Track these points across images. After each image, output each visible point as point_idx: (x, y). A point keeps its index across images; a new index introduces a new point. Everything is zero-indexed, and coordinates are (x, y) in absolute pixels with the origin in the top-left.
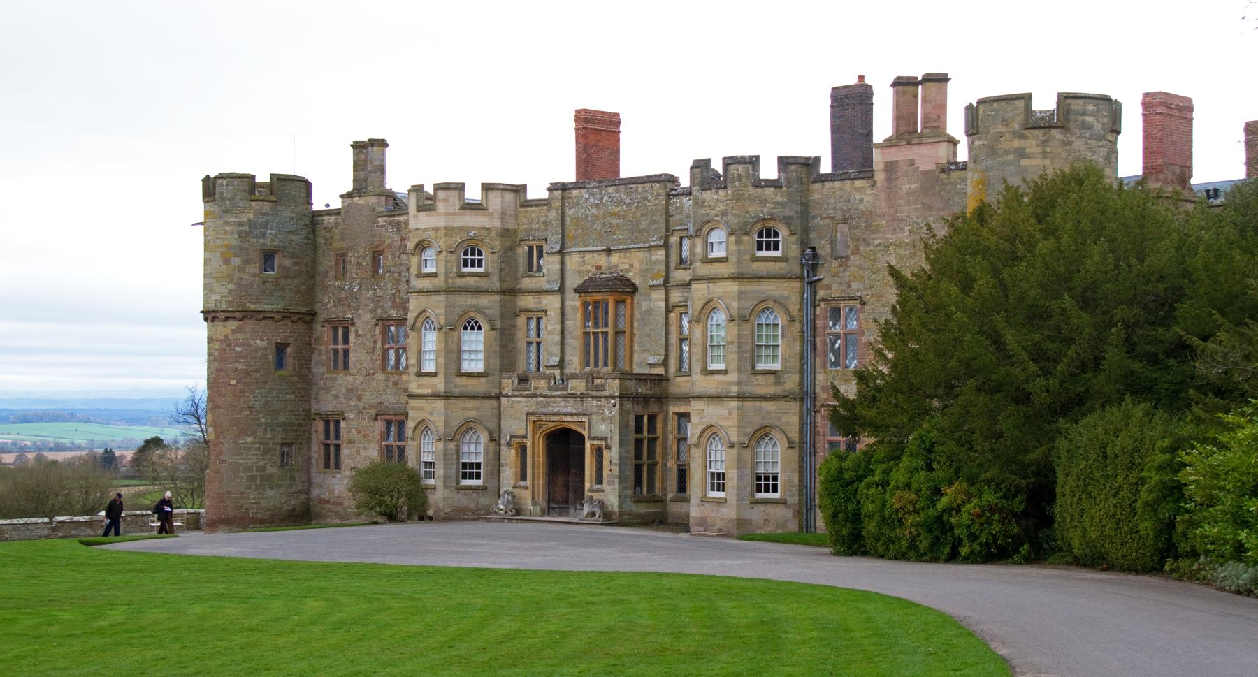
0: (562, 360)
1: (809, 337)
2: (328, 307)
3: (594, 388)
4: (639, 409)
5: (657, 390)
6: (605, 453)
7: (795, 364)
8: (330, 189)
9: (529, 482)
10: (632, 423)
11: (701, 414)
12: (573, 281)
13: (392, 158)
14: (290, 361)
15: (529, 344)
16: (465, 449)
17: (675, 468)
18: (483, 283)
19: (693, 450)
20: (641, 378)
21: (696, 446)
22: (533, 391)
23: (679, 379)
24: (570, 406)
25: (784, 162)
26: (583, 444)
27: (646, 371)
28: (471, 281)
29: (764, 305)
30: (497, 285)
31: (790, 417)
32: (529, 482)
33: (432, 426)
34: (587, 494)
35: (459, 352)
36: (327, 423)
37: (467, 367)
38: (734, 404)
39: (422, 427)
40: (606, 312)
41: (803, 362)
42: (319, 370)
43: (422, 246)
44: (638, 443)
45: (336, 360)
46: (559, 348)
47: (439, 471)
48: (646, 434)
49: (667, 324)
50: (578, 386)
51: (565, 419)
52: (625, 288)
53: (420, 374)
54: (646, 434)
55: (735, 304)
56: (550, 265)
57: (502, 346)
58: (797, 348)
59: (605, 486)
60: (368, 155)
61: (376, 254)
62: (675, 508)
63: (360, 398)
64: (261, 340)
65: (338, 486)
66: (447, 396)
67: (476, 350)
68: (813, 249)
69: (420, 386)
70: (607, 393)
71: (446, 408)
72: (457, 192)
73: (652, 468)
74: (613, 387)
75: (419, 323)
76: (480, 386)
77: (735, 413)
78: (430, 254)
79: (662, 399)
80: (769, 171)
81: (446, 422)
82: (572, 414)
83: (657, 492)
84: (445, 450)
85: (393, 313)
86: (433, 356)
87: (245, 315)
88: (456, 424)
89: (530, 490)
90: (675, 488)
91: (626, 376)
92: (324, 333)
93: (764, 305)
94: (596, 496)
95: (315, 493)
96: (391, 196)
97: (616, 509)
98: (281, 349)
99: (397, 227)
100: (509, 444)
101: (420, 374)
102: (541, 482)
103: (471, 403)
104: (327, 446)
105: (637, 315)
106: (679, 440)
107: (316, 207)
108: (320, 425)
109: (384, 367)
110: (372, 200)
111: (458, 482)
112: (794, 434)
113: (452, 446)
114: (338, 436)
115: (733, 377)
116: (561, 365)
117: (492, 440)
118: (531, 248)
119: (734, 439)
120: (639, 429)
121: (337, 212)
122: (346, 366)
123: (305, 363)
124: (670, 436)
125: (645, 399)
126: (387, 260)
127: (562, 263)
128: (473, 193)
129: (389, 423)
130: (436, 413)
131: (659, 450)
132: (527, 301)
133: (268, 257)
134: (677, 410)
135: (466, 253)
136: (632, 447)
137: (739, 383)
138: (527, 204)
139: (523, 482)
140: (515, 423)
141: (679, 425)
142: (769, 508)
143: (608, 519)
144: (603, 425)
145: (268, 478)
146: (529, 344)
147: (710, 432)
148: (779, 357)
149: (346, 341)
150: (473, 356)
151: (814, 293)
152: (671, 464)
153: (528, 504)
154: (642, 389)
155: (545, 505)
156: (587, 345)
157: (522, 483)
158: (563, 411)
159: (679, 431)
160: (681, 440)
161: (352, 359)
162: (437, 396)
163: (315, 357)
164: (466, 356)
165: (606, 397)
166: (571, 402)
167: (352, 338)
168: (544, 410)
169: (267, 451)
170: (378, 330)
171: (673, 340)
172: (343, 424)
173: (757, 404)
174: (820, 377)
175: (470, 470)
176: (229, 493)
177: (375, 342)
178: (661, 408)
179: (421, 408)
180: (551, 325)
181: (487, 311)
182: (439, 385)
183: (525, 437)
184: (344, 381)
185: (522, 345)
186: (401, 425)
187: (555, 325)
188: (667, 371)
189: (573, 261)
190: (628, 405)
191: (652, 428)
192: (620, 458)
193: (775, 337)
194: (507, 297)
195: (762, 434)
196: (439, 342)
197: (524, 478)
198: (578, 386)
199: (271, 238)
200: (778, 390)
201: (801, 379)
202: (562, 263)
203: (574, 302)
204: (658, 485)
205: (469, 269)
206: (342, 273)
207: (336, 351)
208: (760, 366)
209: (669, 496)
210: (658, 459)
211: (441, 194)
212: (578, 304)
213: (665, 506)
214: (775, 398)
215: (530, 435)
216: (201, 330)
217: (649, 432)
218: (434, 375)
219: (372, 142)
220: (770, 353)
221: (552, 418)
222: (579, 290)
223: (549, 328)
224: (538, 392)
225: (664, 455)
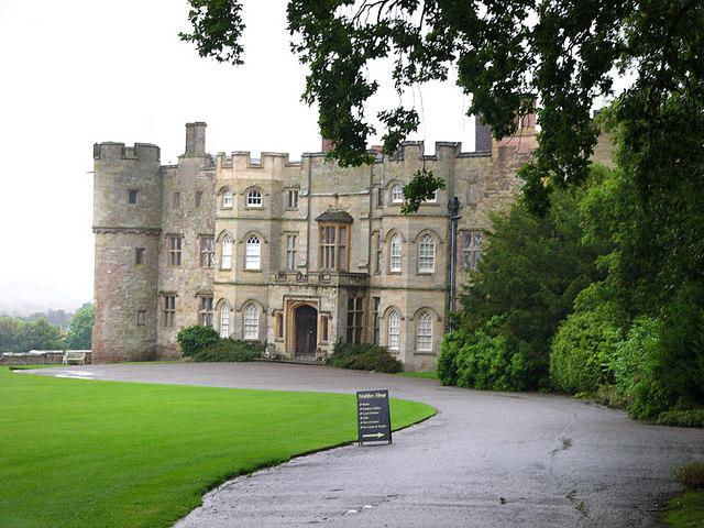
0: (308, 263)
1: (452, 251)
2: (170, 226)
3: (321, 284)
5: (362, 283)
7: (444, 267)
8: (171, 154)
9: (284, 338)
10: (346, 304)
11: (387, 299)
12: (315, 214)
13: (209, 134)
14: (144, 260)
15: (289, 252)
18: (260, 214)
20: (354, 276)
21: (383, 318)
24: (310, 292)
25: (439, 145)
27: (358, 271)
28: (253, 213)
29: (425, 233)
30: (268, 214)
31: (438, 302)
32: (284, 338)
36: (167, 298)
37: (249, 266)
38: (405, 293)
39: (221, 303)
40: (334, 233)
41: (449, 267)
42: (163, 265)
43: (224, 190)
44: (350, 316)
45: (173, 260)
49: (370, 242)
50: (314, 279)
52: (345, 220)
53: (221, 270)
55: (407, 232)
56: (302, 204)
58: (444, 259)
60: (195, 131)
61: (199, 194)
63: (187, 283)
64: (127, 245)
65: (171, 337)
66: (236, 284)
67: (255, 255)
68: (456, 198)
70: (332, 284)
72: (244, 159)
75: (221, 237)
76: (257, 278)
77: (405, 299)
78: (228, 196)
79: (366, 288)
80: (430, 150)
85: (209, 231)
86: (229, 259)
87: (117, 230)
91: (343, 273)
92: (166, 242)
93: (425, 233)
95: (159, 342)
96: (209, 157)
98: (139, 252)
99: (211, 177)
101: (221, 270)
102: (291, 338)
103: (252, 288)
104: (167, 313)
105: (353, 236)
107: (164, 162)
108: (163, 299)
109: (201, 265)
110: (197, 160)
112: (442, 313)
113: (239, 314)
114: (173, 307)
115: (405, 276)
116: (307, 266)
117: (264, 311)
118: (291, 192)
119: (405, 315)
120: (351, 306)
121: (176, 167)
122: (179, 264)
123: (155, 261)
126: (205, 196)
127: (309, 202)
128: (256, 156)
129: (204, 299)
130: (229, 294)
132: (289, 226)
133: (133, 194)
135: (250, 195)
136: (346, 319)
137: (409, 280)
138: (289, 165)
142: (425, 358)
143: (329, 362)
144: (329, 303)
145: (131, 332)
146: (289, 252)
147: (391, 310)
148: (434, 266)
149: (179, 248)
150: (253, 259)
151: (456, 226)
152: (371, 329)
156: (322, 258)
158: (305, 293)
161: (182, 260)
162: (231, 284)
163: (161, 257)
164: (249, 259)
167: (183, 245)
169: (129, 315)
170: (198, 241)
171: (374, 252)
172: (176, 299)
173: (423, 293)
174: (458, 278)
176: (106, 340)
180: (302, 241)
181: (262, 232)
182: (233, 277)
184: (177, 271)
185: (284, 252)
186: (211, 300)
187: (305, 246)
189: (316, 202)
190: (344, 292)
193: (432, 252)
194: (275, 223)
195: (422, 312)
197: (281, 336)
199: (134, 182)
200: (433, 286)
201: (448, 279)
202: (309, 202)
203: (315, 226)
205: (252, 205)
206: (177, 204)
207: (173, 253)
208: (421, 270)
211: (235, 158)
212: (317, 228)
214: (430, 290)
216: (91, 239)
219: (198, 124)
220: (428, 262)
222: (319, 220)
223: (301, 243)
224: (291, 283)
225: (366, 324)
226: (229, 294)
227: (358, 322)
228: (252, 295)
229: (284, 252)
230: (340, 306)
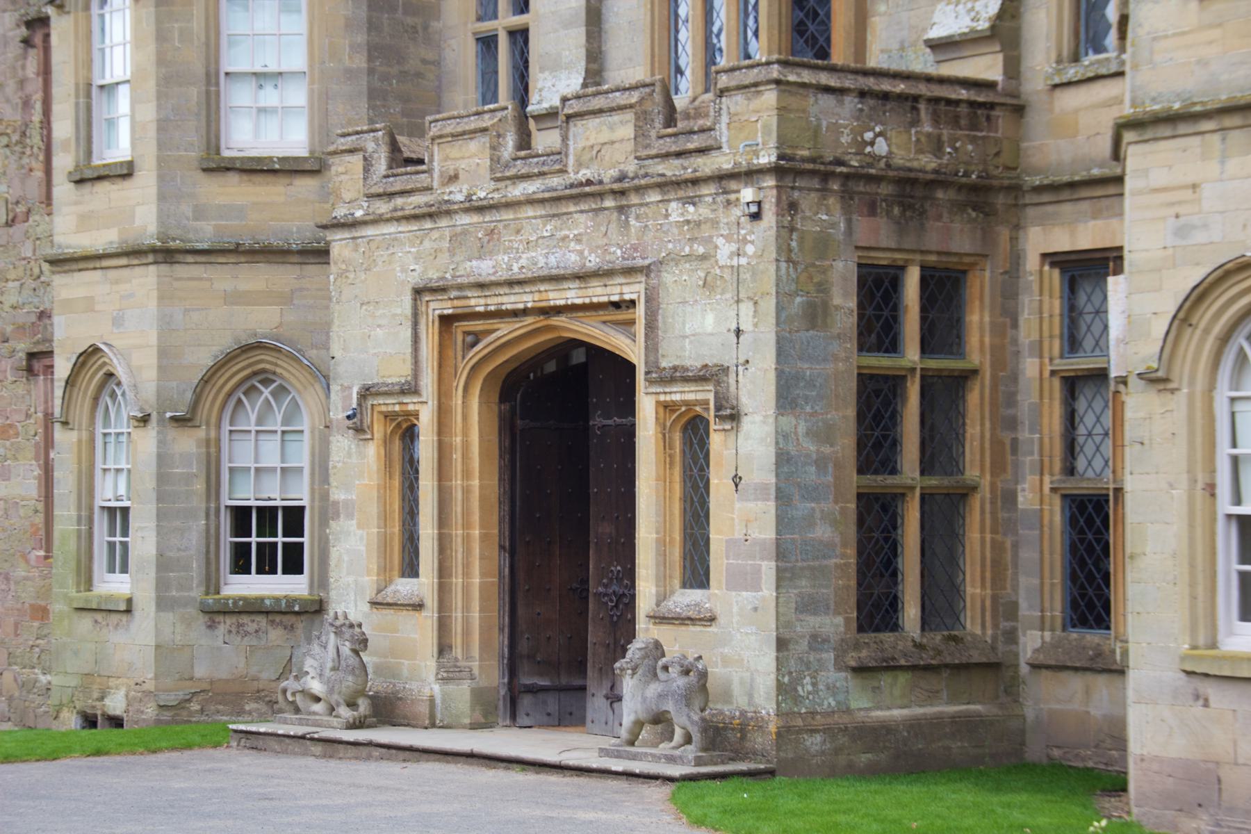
4: (878, 234)
5: (963, 152)
6: (716, 440)
9: (424, 585)
10: (844, 301)
16: (241, 454)
17: (1055, 515)
19: (1139, 406)
20: (893, 96)
21: (1157, 380)
23: (1071, 100)
24: (576, 242)
26: (628, 406)
27: (923, 63)
33: (121, 372)
34: (646, 631)
35: (213, 80)
37: (245, 136)
44: (876, 400)
46: (578, 35)
47: (143, 541)
48: (911, 353)
50: (607, 145)
51: (557, 297)
54: (911, 353)
57: (374, 51)
59: (715, 597)
62: (1056, 700)
69: (86, 221)
70: (722, 162)
71: (164, 297)
73: (945, 512)
74: (750, 129)
76: (282, 211)
79: (994, 196)
81: (163, 353)
82: (582, 277)
83: (974, 624)
84: (162, 459)
88: (204, 358)
89: (428, 618)
90: (1056, 607)
94: (677, 643)
97: (765, 703)
106: (1073, 385)
111: (212, 583)
113: (187, 443)
120: (878, 326)
124: (1030, 367)
125: (910, 193)
131: (976, 428)
134: (1062, 241)
136: (844, 416)
139: (403, 586)
140: (371, 326)
141: (1072, 314)
144: (717, 310)
150: (269, 96)
152: (1038, 497)
153: (423, 678)
154: (890, 145)
155: (493, 677)
157: (404, 588)
158: (540, 256)
159: (1073, 343)
160: (1084, 385)
162: (134, 253)
164: (239, 96)
165: (721, 178)
166: (580, 222)
168: (484, 268)
175: (270, 536)
177: (27, 104)
178: (987, 237)
179: (89, 305)
182: (138, 211)
183: (410, 389)
188: (1013, 67)
190: (824, 214)
191: (942, 329)
192: (783, 459)
196: (137, 43)
197: (411, 569)
198: (607, 145)
204: (974, 589)
209: (1031, 642)
210: (974, 469)
213: (1012, 689)
217: (926, 348)
218: (126, 172)
225: (1004, 455)
226: (127, 323)
227: (940, 448)
228: (261, 320)
229: (461, 55)
230: (801, 316)
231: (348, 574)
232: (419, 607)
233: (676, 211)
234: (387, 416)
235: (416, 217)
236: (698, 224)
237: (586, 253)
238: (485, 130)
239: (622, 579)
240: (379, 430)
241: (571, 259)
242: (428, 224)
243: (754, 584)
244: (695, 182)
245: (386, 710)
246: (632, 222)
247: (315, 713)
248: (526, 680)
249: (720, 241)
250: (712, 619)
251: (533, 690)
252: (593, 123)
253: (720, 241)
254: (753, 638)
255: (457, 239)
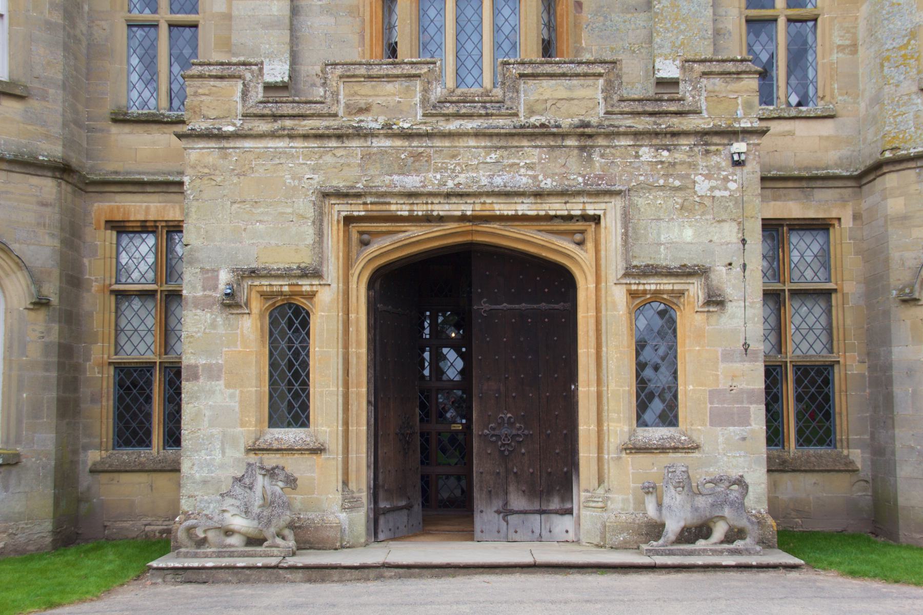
22: (345, 120)
24: (530, 167)
82: (564, 194)
100: (231, 302)
143: (684, 545)
168: (412, 182)
215: (332, 270)
221: (440, 208)
231: (211, 425)
232: (318, 451)
233: (646, 153)
234: (265, 296)
235: (305, 137)
236: (673, 165)
237: (541, 177)
238: (418, 76)
239: (514, 423)
240: (256, 305)
241: (523, 181)
242: (333, 143)
243: (743, 419)
244: (674, 134)
245: (306, 537)
246: (596, 157)
247: (230, 546)
248: (383, 505)
249: (699, 179)
250: (697, 447)
251: (386, 512)
252: (546, 83)
253: (699, 179)
254: (742, 459)
255: (367, 157)
